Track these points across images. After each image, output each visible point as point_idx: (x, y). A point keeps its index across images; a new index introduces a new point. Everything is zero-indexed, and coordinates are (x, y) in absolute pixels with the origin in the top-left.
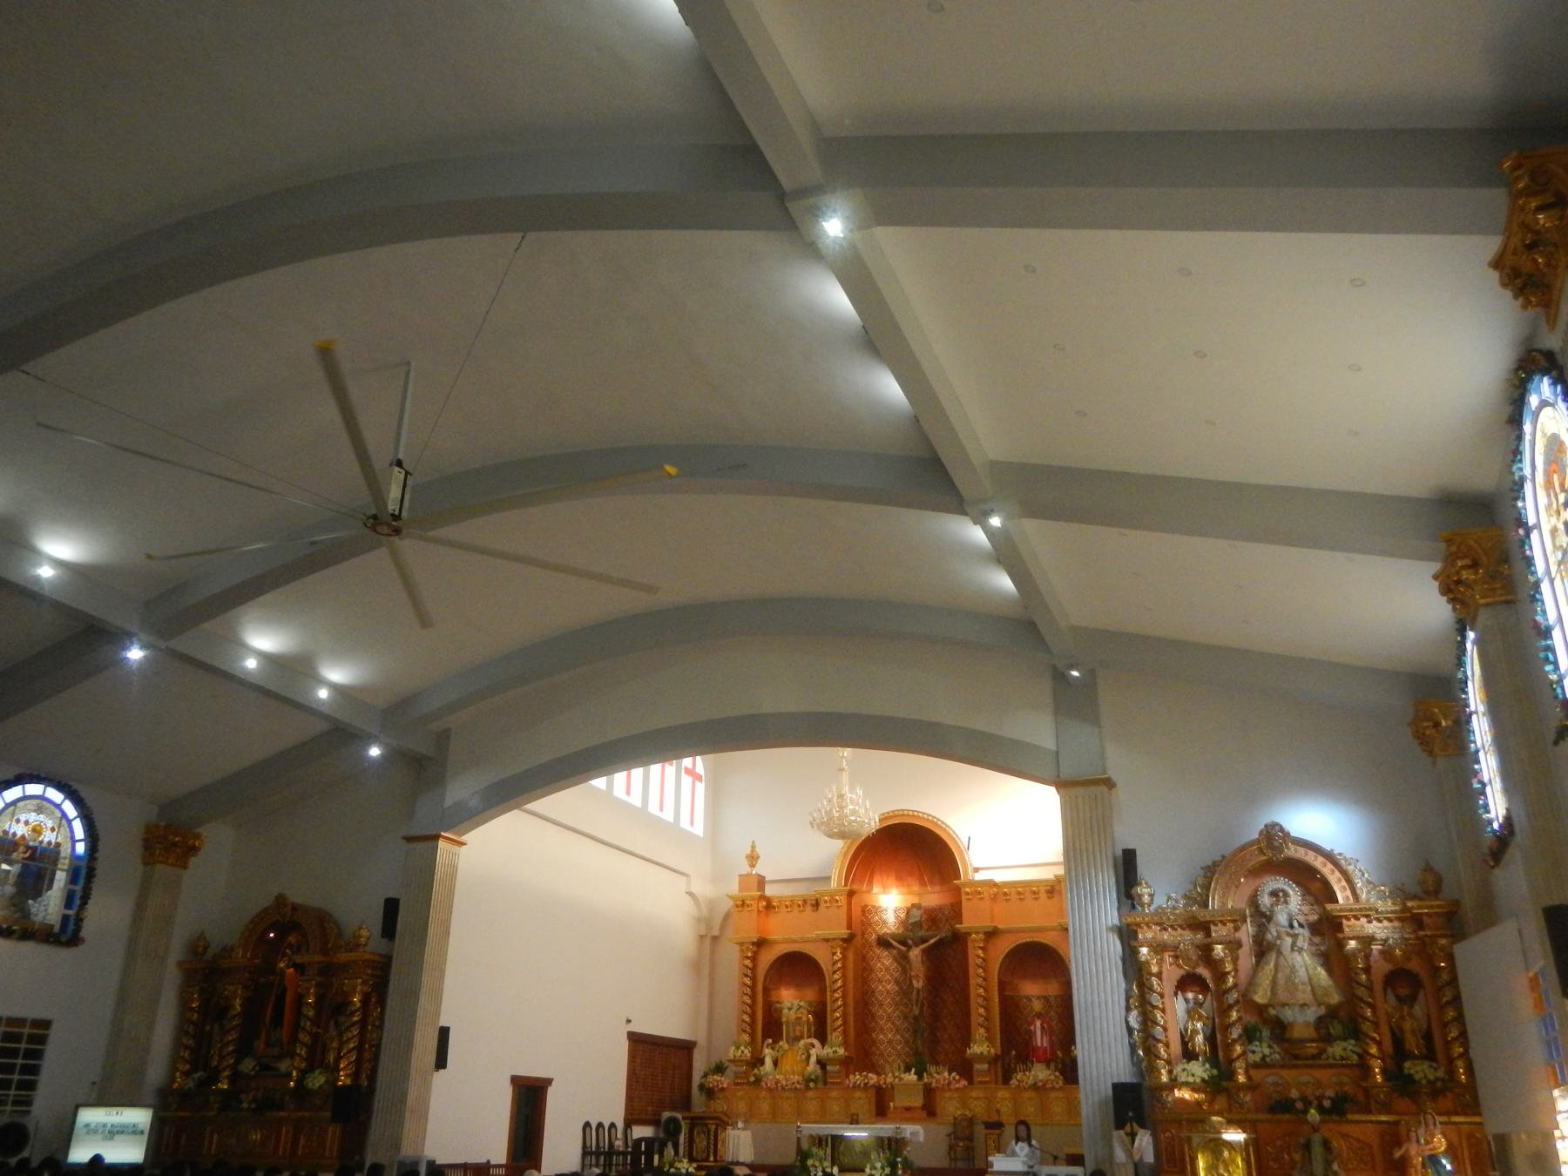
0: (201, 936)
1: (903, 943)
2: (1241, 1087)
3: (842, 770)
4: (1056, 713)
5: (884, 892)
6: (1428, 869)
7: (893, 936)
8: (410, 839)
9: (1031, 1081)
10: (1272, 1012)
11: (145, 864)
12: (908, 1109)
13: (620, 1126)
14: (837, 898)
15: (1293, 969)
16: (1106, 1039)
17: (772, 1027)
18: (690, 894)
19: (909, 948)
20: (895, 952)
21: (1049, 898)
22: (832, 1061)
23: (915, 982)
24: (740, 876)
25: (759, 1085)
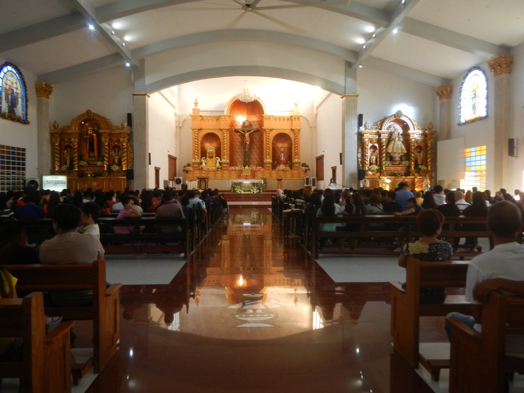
0: (55, 122)
1: (243, 131)
2: (384, 170)
3: (246, 81)
4: (346, 75)
5: (237, 117)
6: (431, 124)
7: (240, 129)
8: (134, 95)
9: (282, 169)
10: (392, 154)
11: (38, 97)
12: (247, 176)
13: (168, 180)
14: (226, 118)
15: (398, 145)
16: (352, 160)
17: (204, 153)
18: (175, 114)
19: (245, 133)
20: (239, 134)
21: (288, 121)
22: (224, 163)
23: (247, 143)
24: (193, 109)
25: (202, 170)
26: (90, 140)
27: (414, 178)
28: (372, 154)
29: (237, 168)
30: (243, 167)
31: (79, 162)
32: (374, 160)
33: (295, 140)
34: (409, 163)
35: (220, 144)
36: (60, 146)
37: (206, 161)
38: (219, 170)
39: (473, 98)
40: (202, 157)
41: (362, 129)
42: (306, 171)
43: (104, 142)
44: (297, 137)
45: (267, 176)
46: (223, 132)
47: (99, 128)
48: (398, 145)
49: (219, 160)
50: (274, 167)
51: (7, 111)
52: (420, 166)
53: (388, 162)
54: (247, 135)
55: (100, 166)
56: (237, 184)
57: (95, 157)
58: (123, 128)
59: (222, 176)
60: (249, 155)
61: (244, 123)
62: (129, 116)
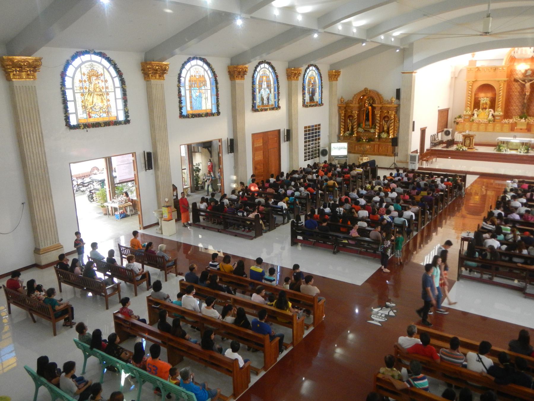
0: (342, 98)
1: (524, 81)
7: (520, 79)
11: (330, 81)
12: (521, 129)
17: (477, 105)
19: (526, 83)
22: (497, 116)
26: (366, 111)
29: (511, 121)
30: (519, 119)
35: (495, 94)
36: (345, 116)
37: (478, 113)
38: (491, 122)
40: (474, 108)
46: (500, 83)
47: (374, 102)
51: (309, 101)
56: (503, 143)
57: (369, 125)
58: (391, 102)
59: (494, 129)
61: (526, 71)
62: (398, 91)
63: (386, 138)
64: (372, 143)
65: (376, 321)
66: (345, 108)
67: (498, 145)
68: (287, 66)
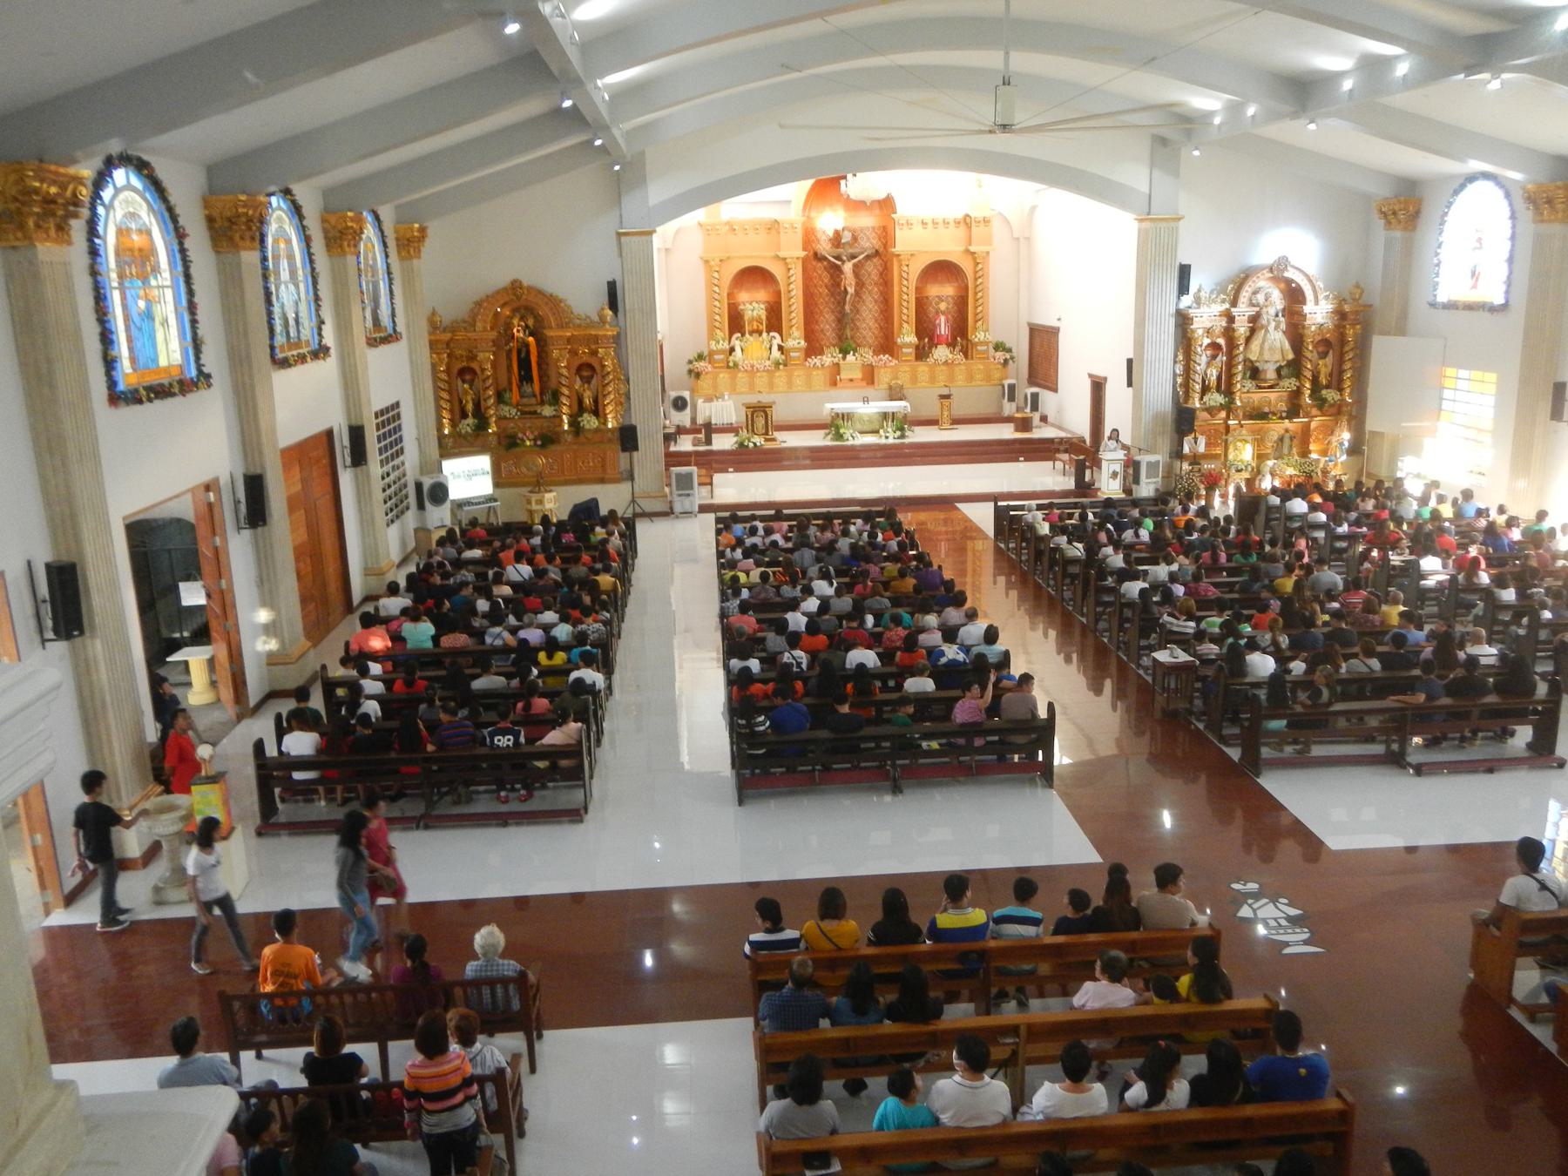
0: (434, 314)
1: (838, 258)
4: (1152, 165)
6: (1357, 286)
10: (1257, 364)
12: (851, 380)
17: (736, 323)
19: (843, 262)
22: (795, 350)
23: (849, 289)
26: (519, 352)
27: (1309, 422)
28: (1209, 364)
30: (840, 355)
31: (497, 410)
32: (1214, 378)
33: (976, 279)
34: (1297, 384)
35: (779, 294)
36: (448, 372)
38: (781, 367)
39: (1475, 248)
41: (1186, 301)
42: (1006, 361)
43: (558, 360)
44: (980, 273)
45: (904, 379)
46: (786, 264)
47: (538, 319)
48: (1273, 345)
49: (777, 341)
50: (921, 353)
51: (371, 325)
52: (1324, 392)
53: (1249, 384)
54: (848, 267)
55: (550, 417)
57: (535, 396)
59: (790, 384)
60: (852, 320)
61: (837, 235)
62: (612, 288)
63: (597, 431)
64: (553, 448)
65: (1297, 943)
66: (448, 344)
67: (834, 424)
68: (322, 203)
